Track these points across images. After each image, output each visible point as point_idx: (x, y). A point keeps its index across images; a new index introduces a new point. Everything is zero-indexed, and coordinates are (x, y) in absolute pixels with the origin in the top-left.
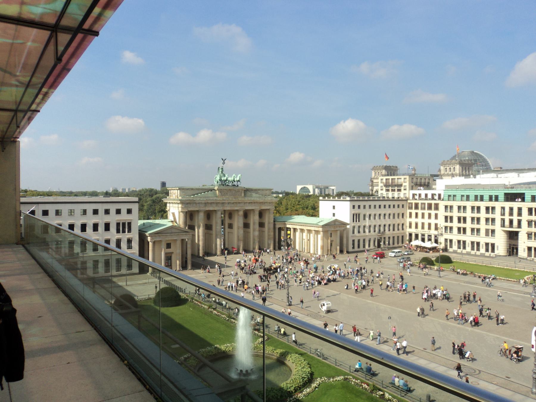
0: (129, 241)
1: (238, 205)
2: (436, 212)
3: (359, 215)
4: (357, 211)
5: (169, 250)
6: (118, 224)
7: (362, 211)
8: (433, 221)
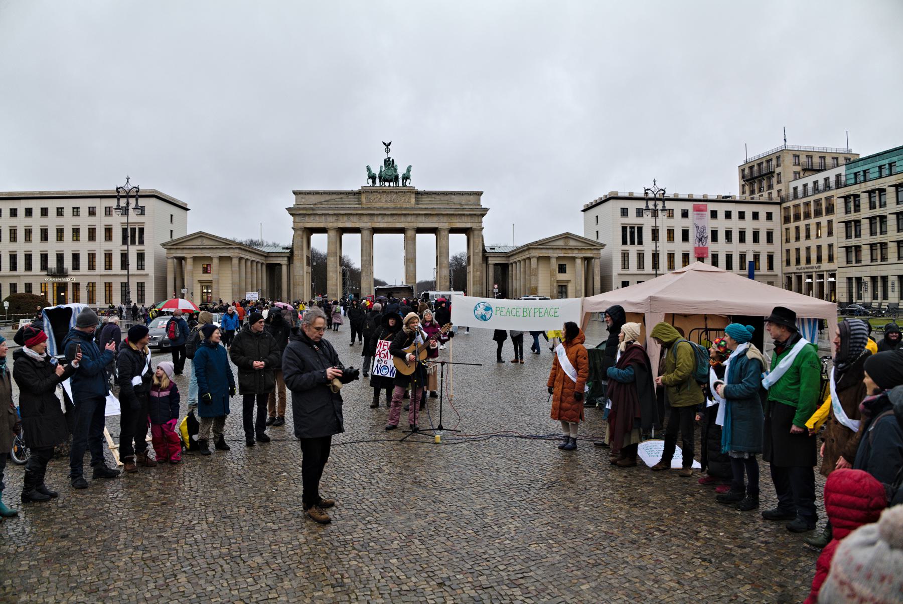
0: (141, 256)
1: (403, 219)
2: (829, 217)
3: (640, 229)
4: (632, 219)
5: (206, 277)
6: (125, 231)
7: (647, 222)
8: (825, 241)
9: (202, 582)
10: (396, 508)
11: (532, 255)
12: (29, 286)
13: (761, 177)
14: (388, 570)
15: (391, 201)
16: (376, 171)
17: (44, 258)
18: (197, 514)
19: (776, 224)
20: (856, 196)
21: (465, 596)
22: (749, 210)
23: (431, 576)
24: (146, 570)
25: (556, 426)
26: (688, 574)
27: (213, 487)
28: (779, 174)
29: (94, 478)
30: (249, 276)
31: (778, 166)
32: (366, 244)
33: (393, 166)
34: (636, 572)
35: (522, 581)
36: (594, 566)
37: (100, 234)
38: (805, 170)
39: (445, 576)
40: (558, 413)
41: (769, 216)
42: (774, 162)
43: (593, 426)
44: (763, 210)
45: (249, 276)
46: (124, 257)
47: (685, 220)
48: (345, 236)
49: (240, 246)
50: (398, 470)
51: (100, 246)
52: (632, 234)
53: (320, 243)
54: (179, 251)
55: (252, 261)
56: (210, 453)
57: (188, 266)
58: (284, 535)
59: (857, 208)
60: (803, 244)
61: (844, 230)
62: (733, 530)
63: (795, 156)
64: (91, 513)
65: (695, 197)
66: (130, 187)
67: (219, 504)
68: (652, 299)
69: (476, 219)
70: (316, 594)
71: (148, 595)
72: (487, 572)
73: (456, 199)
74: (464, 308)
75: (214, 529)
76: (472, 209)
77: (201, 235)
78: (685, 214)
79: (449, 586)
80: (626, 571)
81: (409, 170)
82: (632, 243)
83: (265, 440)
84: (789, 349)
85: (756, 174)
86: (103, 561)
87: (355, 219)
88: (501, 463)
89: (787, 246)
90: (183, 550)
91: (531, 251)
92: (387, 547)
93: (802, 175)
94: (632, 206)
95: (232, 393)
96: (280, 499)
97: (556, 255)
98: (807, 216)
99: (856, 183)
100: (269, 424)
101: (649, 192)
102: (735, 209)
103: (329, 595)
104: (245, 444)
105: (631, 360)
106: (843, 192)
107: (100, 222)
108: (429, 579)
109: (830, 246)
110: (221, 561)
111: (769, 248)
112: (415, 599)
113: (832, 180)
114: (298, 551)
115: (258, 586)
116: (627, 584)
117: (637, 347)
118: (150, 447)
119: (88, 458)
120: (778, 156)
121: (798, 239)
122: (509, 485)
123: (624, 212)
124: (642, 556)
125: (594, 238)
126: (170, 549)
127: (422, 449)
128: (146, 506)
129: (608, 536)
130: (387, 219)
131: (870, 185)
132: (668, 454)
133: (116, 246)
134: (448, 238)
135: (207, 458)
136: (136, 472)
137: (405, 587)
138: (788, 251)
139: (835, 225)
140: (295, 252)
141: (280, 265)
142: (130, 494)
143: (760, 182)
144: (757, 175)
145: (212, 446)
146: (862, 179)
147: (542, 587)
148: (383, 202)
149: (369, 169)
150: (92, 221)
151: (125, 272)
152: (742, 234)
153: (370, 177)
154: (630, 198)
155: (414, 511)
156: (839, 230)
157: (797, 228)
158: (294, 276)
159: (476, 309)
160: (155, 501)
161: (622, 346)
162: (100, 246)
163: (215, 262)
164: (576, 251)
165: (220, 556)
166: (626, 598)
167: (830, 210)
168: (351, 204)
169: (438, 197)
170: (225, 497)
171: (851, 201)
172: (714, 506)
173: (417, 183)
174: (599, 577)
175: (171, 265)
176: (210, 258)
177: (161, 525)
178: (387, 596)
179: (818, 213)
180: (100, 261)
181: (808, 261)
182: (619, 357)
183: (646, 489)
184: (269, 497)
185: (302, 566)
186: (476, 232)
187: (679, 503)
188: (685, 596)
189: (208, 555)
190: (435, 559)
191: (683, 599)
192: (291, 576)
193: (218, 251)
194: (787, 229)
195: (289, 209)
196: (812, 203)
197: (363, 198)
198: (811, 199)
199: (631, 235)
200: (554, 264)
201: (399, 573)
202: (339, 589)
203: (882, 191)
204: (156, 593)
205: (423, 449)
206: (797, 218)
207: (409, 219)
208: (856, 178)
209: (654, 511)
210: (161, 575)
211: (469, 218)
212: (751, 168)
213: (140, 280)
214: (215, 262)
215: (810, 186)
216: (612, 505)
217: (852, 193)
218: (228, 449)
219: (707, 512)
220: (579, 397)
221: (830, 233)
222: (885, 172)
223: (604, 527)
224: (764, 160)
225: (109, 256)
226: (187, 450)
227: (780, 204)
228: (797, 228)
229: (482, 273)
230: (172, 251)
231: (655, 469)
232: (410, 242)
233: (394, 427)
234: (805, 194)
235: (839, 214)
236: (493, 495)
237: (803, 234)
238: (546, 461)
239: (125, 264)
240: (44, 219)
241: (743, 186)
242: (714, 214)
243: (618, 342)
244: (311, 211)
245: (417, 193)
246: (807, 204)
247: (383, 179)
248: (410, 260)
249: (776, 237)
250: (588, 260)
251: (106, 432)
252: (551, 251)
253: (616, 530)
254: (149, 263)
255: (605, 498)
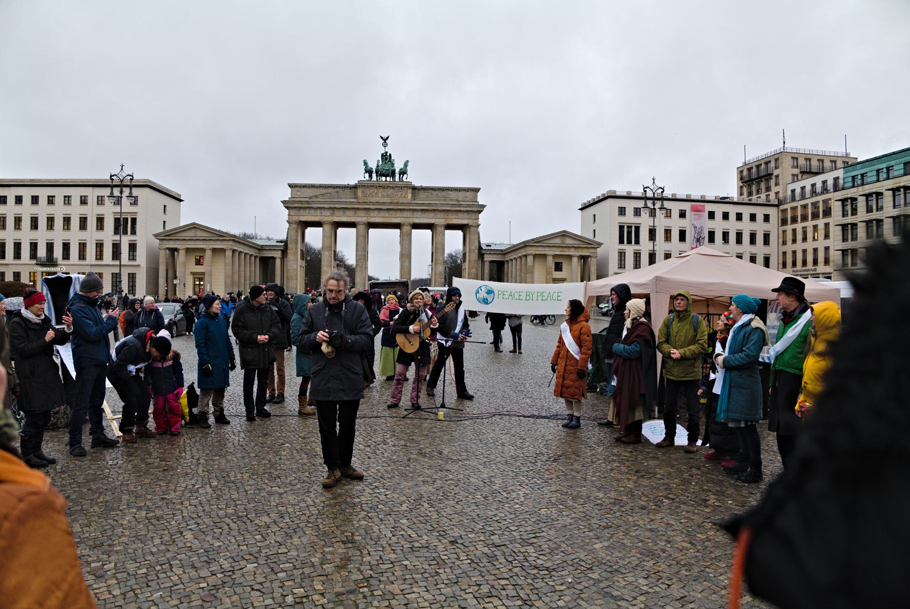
0: (133, 247)
1: (399, 214)
2: (826, 220)
3: (637, 229)
4: (630, 218)
5: (199, 269)
6: (117, 221)
7: (645, 222)
8: (821, 244)
9: (209, 538)
10: (403, 476)
11: (529, 252)
12: (17, 275)
13: (759, 178)
14: (399, 529)
15: (388, 196)
16: (373, 165)
17: (34, 246)
18: (200, 479)
19: (773, 227)
20: (854, 200)
21: (478, 553)
22: (746, 211)
23: (442, 535)
24: (151, 527)
25: (560, 406)
26: (700, 535)
27: (215, 456)
28: (777, 176)
29: (92, 447)
30: (242, 268)
31: (776, 168)
32: (361, 239)
33: (390, 161)
34: (648, 534)
35: (535, 540)
36: (605, 528)
37: (92, 223)
38: (803, 173)
39: (456, 535)
40: (561, 392)
41: (767, 218)
42: (772, 164)
43: (596, 407)
44: (760, 212)
45: (242, 268)
46: (116, 247)
47: (682, 221)
48: (340, 231)
49: (234, 239)
50: (402, 442)
51: (91, 236)
52: (629, 233)
53: (314, 237)
54: (171, 242)
55: (246, 254)
56: (209, 427)
57: (181, 257)
58: (291, 498)
59: (854, 211)
60: (799, 246)
61: (840, 233)
62: (740, 499)
63: (793, 158)
64: (90, 477)
65: (692, 198)
66: (124, 175)
67: (222, 471)
68: (658, 279)
69: (473, 216)
70: (327, 550)
71: (154, 550)
72: (499, 532)
73: (453, 195)
74: (469, 288)
75: (219, 493)
76: (469, 206)
77: (194, 227)
78: (682, 215)
79: (462, 544)
80: (637, 532)
81: (406, 165)
82: (629, 242)
83: (267, 415)
84: (798, 318)
85: (754, 176)
86: (106, 519)
87: (350, 213)
88: (506, 439)
89: (783, 248)
90: (188, 509)
91: (528, 248)
92: (396, 509)
93: (800, 177)
94: (630, 205)
95: (233, 367)
96: (284, 467)
97: (552, 253)
98: (804, 218)
99: (853, 187)
100: (269, 402)
101: (648, 190)
102: (733, 210)
103: (340, 551)
104: (245, 418)
105: (637, 336)
106: (841, 195)
107: (92, 211)
108: (441, 538)
109: (827, 249)
110: (227, 520)
111: (766, 250)
112: (429, 554)
113: (830, 183)
114: (307, 512)
115: (267, 542)
116: (640, 544)
117: (643, 323)
118: (151, 419)
119: (87, 428)
120: (777, 158)
121: (794, 241)
122: (515, 458)
123: (622, 211)
124: (652, 520)
125: (591, 237)
126: (175, 510)
127: (425, 425)
128: (147, 472)
129: (617, 502)
130: (382, 214)
131: (867, 189)
132: (670, 433)
133: (108, 236)
134: (444, 235)
135: (207, 431)
136: (136, 442)
137: (417, 544)
138: (784, 253)
139: (832, 228)
140: (290, 246)
141: (274, 258)
142: (130, 461)
143: (758, 184)
144: (756, 177)
145: (211, 420)
146: (860, 182)
147: (555, 545)
148: (380, 197)
149: (365, 163)
150: (84, 210)
151: (117, 263)
152: (739, 235)
153: (366, 172)
154: (629, 197)
155: (421, 479)
156: (836, 232)
157: (794, 231)
158: (288, 270)
159: (477, 292)
160: (157, 467)
161: (628, 323)
162: (91, 236)
163: (208, 254)
164: (573, 250)
165: (226, 516)
166: (639, 556)
167: (827, 212)
168: (347, 198)
169: (435, 193)
170: (228, 465)
171: (849, 204)
172: (720, 478)
173: (414, 178)
174: (611, 538)
175: (163, 256)
176: (203, 250)
177: (164, 488)
178: (399, 551)
179: (815, 216)
180: (91, 251)
181: (804, 263)
182: (625, 333)
183: (652, 463)
184: (272, 466)
185: (310, 525)
186: (472, 229)
187: (686, 476)
188: (698, 554)
189: (213, 514)
190: (446, 520)
191: (696, 557)
192: (301, 533)
193: (212, 242)
194: (784, 232)
195: (284, 202)
196: (810, 206)
197: (360, 192)
198: (809, 201)
199: (629, 234)
200: (551, 262)
201: (410, 532)
202: (350, 545)
203: (879, 195)
204: (163, 548)
205: (426, 424)
206: (794, 220)
207: (405, 214)
208: (853, 181)
209: (662, 481)
210: (166, 532)
211: (466, 215)
212: (750, 170)
213: (132, 270)
214: (208, 254)
215: (808, 188)
216: (619, 476)
217: (849, 196)
218: (228, 423)
219: (714, 483)
220: (582, 374)
221: (827, 236)
222: (883, 176)
223: (613, 495)
224: (763, 162)
225: (100, 246)
226: (186, 423)
227: (777, 206)
228: (794, 231)
229: (477, 270)
230: (165, 242)
231: (659, 446)
232: (405, 238)
233: (394, 406)
234: (803, 197)
235: (837, 216)
236: (499, 465)
237: (799, 237)
238: (550, 437)
239: (116, 254)
240: (35, 207)
241: (741, 187)
242: (712, 215)
243: (625, 320)
244: (306, 205)
245: (414, 188)
246: (805, 207)
247: (380, 174)
248: (406, 256)
249: (773, 239)
250: (584, 258)
251: (105, 406)
252: (547, 249)
253: (625, 498)
254: (141, 253)
255: (612, 470)
